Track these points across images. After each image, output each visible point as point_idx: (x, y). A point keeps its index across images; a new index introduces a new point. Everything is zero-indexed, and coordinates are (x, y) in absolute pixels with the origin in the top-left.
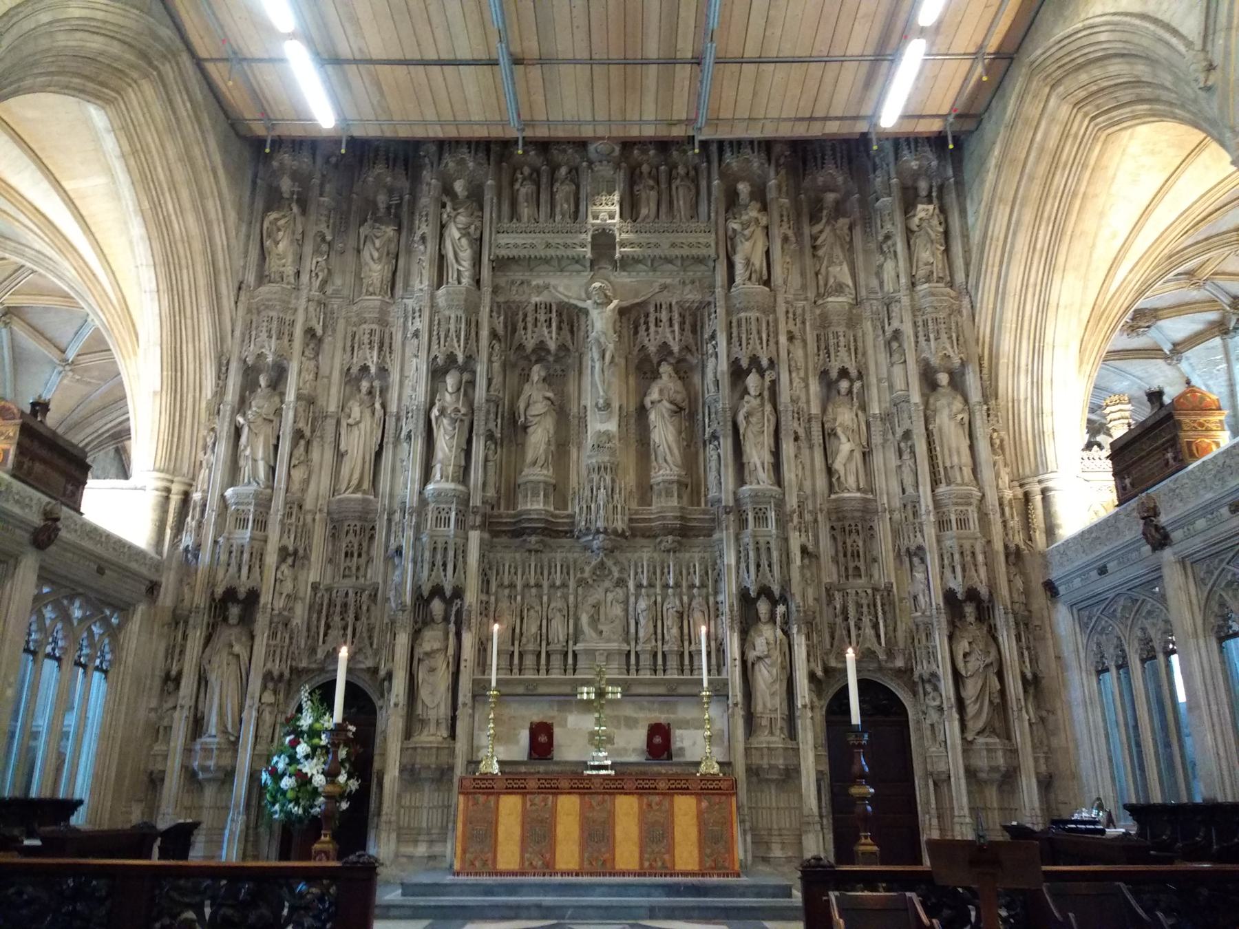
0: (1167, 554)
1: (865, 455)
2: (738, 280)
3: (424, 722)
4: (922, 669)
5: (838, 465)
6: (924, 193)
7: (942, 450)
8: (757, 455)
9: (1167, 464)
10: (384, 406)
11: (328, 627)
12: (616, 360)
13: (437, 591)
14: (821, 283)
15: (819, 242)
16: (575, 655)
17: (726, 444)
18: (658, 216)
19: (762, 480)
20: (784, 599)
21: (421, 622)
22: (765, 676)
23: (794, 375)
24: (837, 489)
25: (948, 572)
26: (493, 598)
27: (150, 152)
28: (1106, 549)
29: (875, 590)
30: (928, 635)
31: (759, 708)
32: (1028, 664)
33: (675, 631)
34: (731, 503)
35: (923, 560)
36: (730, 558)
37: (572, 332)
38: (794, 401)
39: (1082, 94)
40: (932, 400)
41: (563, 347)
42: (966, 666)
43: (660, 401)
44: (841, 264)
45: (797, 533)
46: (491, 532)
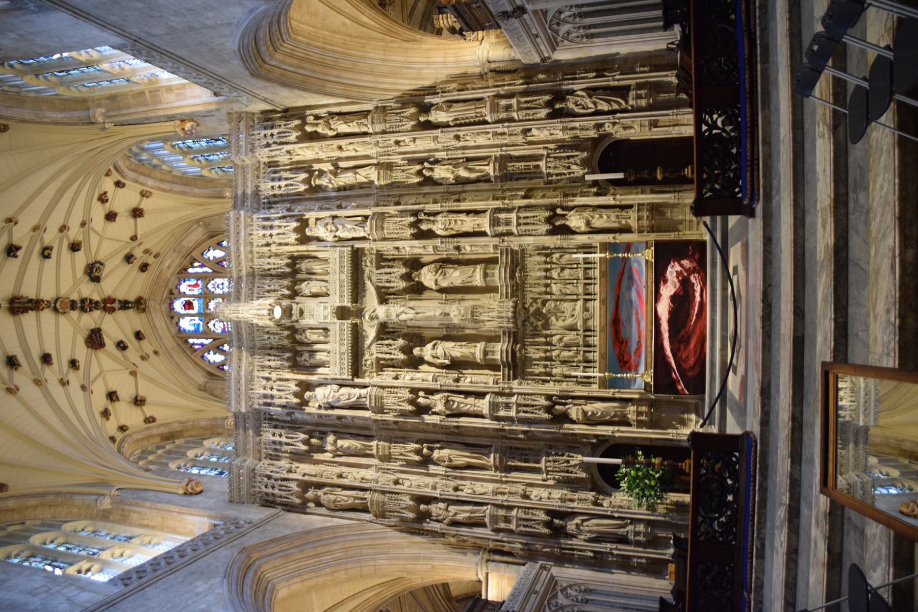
0: (529, 7)
2: (362, 234)
3: (624, 416)
4: (592, 134)
5: (473, 176)
7: (467, 118)
8: (468, 224)
9: (479, 7)
10: (438, 442)
11: (567, 472)
13: (548, 410)
16: (585, 331)
18: (326, 281)
19: (484, 223)
20: (552, 208)
21: (565, 418)
22: (598, 223)
25: (535, 117)
26: (553, 378)
27: (299, 567)
28: (524, 34)
29: (548, 156)
30: (573, 129)
31: (616, 225)
32: (588, 75)
33: (572, 271)
34: (497, 239)
36: (530, 240)
37: (394, 332)
39: (271, 48)
41: (404, 336)
42: (591, 108)
45: (515, 201)
46: (514, 379)
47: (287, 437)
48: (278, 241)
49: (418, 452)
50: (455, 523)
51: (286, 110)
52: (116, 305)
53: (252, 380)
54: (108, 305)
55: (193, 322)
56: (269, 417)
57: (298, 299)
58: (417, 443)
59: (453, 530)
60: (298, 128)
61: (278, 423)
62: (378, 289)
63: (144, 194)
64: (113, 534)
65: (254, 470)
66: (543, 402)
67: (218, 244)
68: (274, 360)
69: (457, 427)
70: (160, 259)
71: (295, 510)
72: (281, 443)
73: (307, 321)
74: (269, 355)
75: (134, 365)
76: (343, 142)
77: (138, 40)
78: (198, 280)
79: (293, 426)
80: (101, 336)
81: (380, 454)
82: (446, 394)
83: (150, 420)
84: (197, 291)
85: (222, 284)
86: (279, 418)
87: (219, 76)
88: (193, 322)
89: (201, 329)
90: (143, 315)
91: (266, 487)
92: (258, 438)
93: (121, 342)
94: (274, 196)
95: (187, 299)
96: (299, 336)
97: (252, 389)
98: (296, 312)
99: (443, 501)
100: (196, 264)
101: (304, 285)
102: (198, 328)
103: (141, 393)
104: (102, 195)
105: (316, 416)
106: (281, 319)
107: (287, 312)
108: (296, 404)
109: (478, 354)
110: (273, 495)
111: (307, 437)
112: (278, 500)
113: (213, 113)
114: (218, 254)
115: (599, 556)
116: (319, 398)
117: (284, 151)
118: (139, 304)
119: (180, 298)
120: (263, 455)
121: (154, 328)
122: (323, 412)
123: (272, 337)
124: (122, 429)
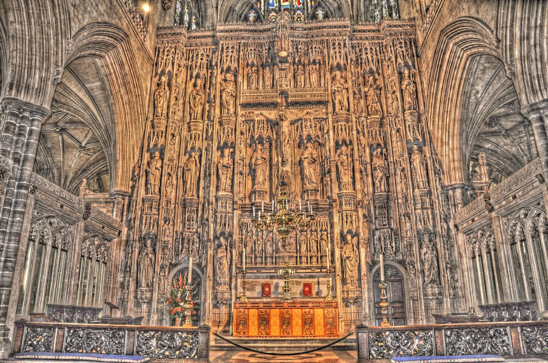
0: (493, 214)
1: (388, 178)
6: (407, 75)
8: (346, 179)
12: (290, 142)
14: (370, 110)
15: (368, 94)
17: (334, 174)
23: (360, 147)
24: (376, 191)
31: (348, 276)
33: (315, 248)
35: (409, 218)
38: (360, 157)
40: (412, 156)
43: (307, 158)
44: (377, 103)
46: (242, 211)
49: (193, 148)
50: (147, 173)
57: (292, 67)
58: (199, 148)
59: (142, 173)
62: (301, 119)
65: (179, 42)
66: (227, 230)
69: (210, 175)
76: (398, 94)
79: (210, 66)
81: (191, 124)
82: (232, 167)
88: (275, 2)
89: (271, 8)
91: (168, 51)
94: (360, 50)
97: (232, 39)
98: (284, 66)
99: (162, 167)
100: (313, 3)
102: (271, 6)
106: (280, 57)
107: (284, 60)
109: (259, 186)
112: (160, 59)
113: (415, 8)
115: (128, 269)
120: (189, 48)
122: (218, 86)
123: (267, 51)
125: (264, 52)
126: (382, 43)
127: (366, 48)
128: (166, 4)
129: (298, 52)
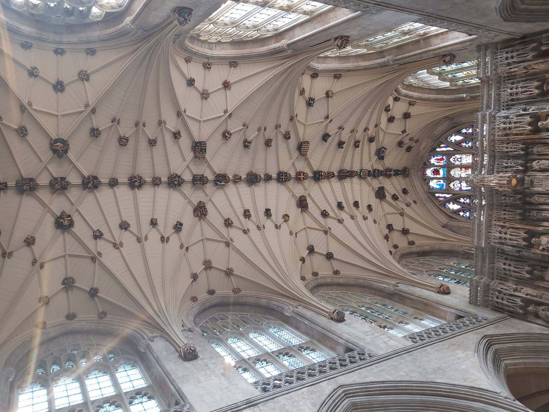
47: (514, 267)
48: (514, 132)
51: (524, 37)
52: (392, 173)
53: (491, 226)
54: (388, 173)
55: (439, 183)
56: (502, 251)
60: (533, 50)
61: (508, 257)
63: (411, 104)
64: (395, 309)
65: (488, 285)
67: (458, 132)
68: (509, 214)
70: (419, 143)
71: (518, 317)
72: (509, 270)
73: (536, 189)
74: (505, 210)
75: (402, 209)
77: (431, 15)
78: (443, 156)
80: (384, 191)
83: (411, 243)
84: (442, 163)
85: (461, 158)
86: (509, 253)
87: (479, 25)
88: (439, 183)
90: (407, 179)
91: (497, 298)
92: (492, 265)
93: (395, 195)
94: (512, 100)
95: (435, 168)
96: (530, 199)
100: (442, 145)
101: (534, 163)
102: (443, 187)
103: (407, 227)
104: (387, 107)
105: (540, 256)
106: (516, 185)
107: (521, 181)
108: (524, 245)
110: (502, 304)
111: (531, 269)
112: (506, 308)
113: (467, 48)
114: (459, 138)
116: (543, 243)
117: (521, 67)
118: (404, 172)
119: (430, 167)
120: (495, 277)
121: (413, 186)
123: (507, 198)
124: (396, 247)
125: (508, 201)
126: (504, 77)
127: (511, 94)
128: (444, 291)
129: (511, 167)
